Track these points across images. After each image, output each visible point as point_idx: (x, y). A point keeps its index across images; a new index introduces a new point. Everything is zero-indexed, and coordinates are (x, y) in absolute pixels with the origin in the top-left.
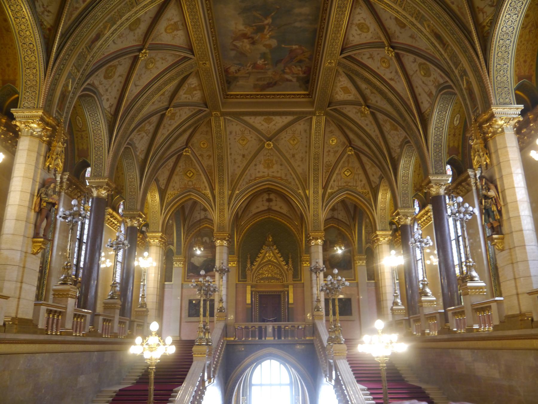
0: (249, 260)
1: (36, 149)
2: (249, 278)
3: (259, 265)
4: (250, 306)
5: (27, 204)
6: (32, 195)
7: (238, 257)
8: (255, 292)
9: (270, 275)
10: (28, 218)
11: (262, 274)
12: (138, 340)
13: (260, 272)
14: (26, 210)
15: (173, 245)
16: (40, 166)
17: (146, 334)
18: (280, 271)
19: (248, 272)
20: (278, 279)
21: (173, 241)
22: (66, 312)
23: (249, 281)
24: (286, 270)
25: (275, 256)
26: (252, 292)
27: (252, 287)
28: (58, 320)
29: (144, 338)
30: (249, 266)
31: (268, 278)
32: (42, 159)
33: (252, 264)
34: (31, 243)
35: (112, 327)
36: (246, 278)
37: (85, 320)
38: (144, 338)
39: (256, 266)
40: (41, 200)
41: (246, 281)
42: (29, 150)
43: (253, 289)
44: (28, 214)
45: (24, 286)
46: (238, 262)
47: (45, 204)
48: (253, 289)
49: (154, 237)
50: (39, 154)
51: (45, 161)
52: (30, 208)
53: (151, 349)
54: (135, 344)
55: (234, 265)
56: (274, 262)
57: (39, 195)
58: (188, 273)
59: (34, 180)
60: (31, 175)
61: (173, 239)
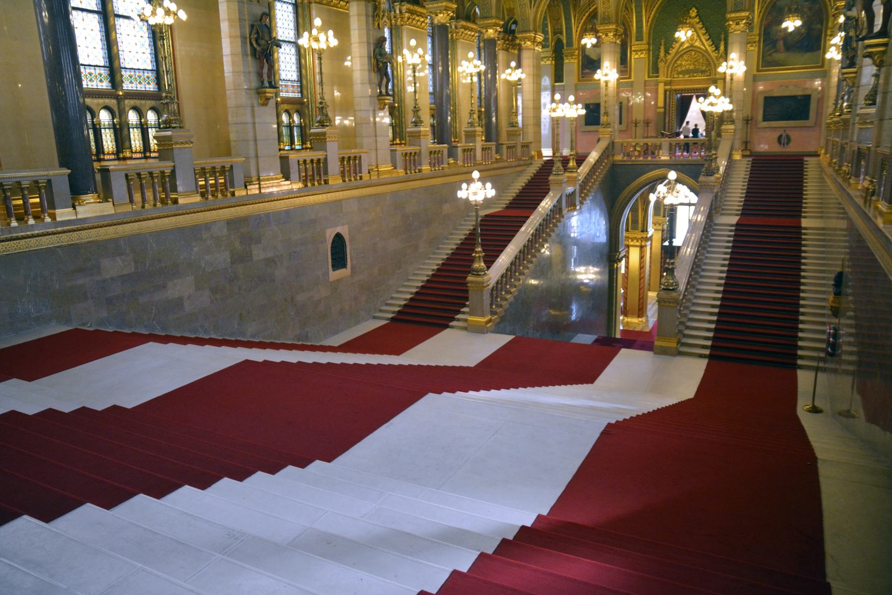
0: (662, 48)
1: (364, 12)
2: (661, 73)
3: (677, 53)
4: (662, 110)
5: (366, 67)
6: (369, 57)
7: (648, 44)
8: (670, 91)
9: (692, 67)
10: (370, 80)
11: (681, 65)
12: (464, 186)
13: (679, 62)
14: (366, 73)
15: (561, 33)
16: (371, 27)
17: (470, 181)
18: (708, 60)
19: (661, 65)
20: (703, 72)
21: (562, 29)
22: (420, 152)
23: (662, 78)
24: (714, 58)
25: (701, 40)
26: (665, 91)
27: (665, 85)
28: (414, 160)
29: (468, 184)
30: (662, 54)
31: (688, 72)
32: (371, 19)
33: (667, 52)
34: (377, 101)
35: (475, 156)
36: (658, 72)
37: (442, 154)
38: (468, 184)
39: (672, 55)
40: (377, 61)
41: (657, 77)
42: (358, 15)
43: (668, 87)
44: (369, 76)
45: (379, 139)
46: (649, 50)
47: (381, 65)
48: (668, 87)
49: (524, 39)
50: (367, 16)
51: (374, 21)
52: (369, 71)
53: (475, 194)
54: (461, 189)
55: (642, 56)
56: (699, 48)
57: (375, 57)
58: (583, 69)
59: (368, 43)
60: (365, 39)
61: (562, 26)
